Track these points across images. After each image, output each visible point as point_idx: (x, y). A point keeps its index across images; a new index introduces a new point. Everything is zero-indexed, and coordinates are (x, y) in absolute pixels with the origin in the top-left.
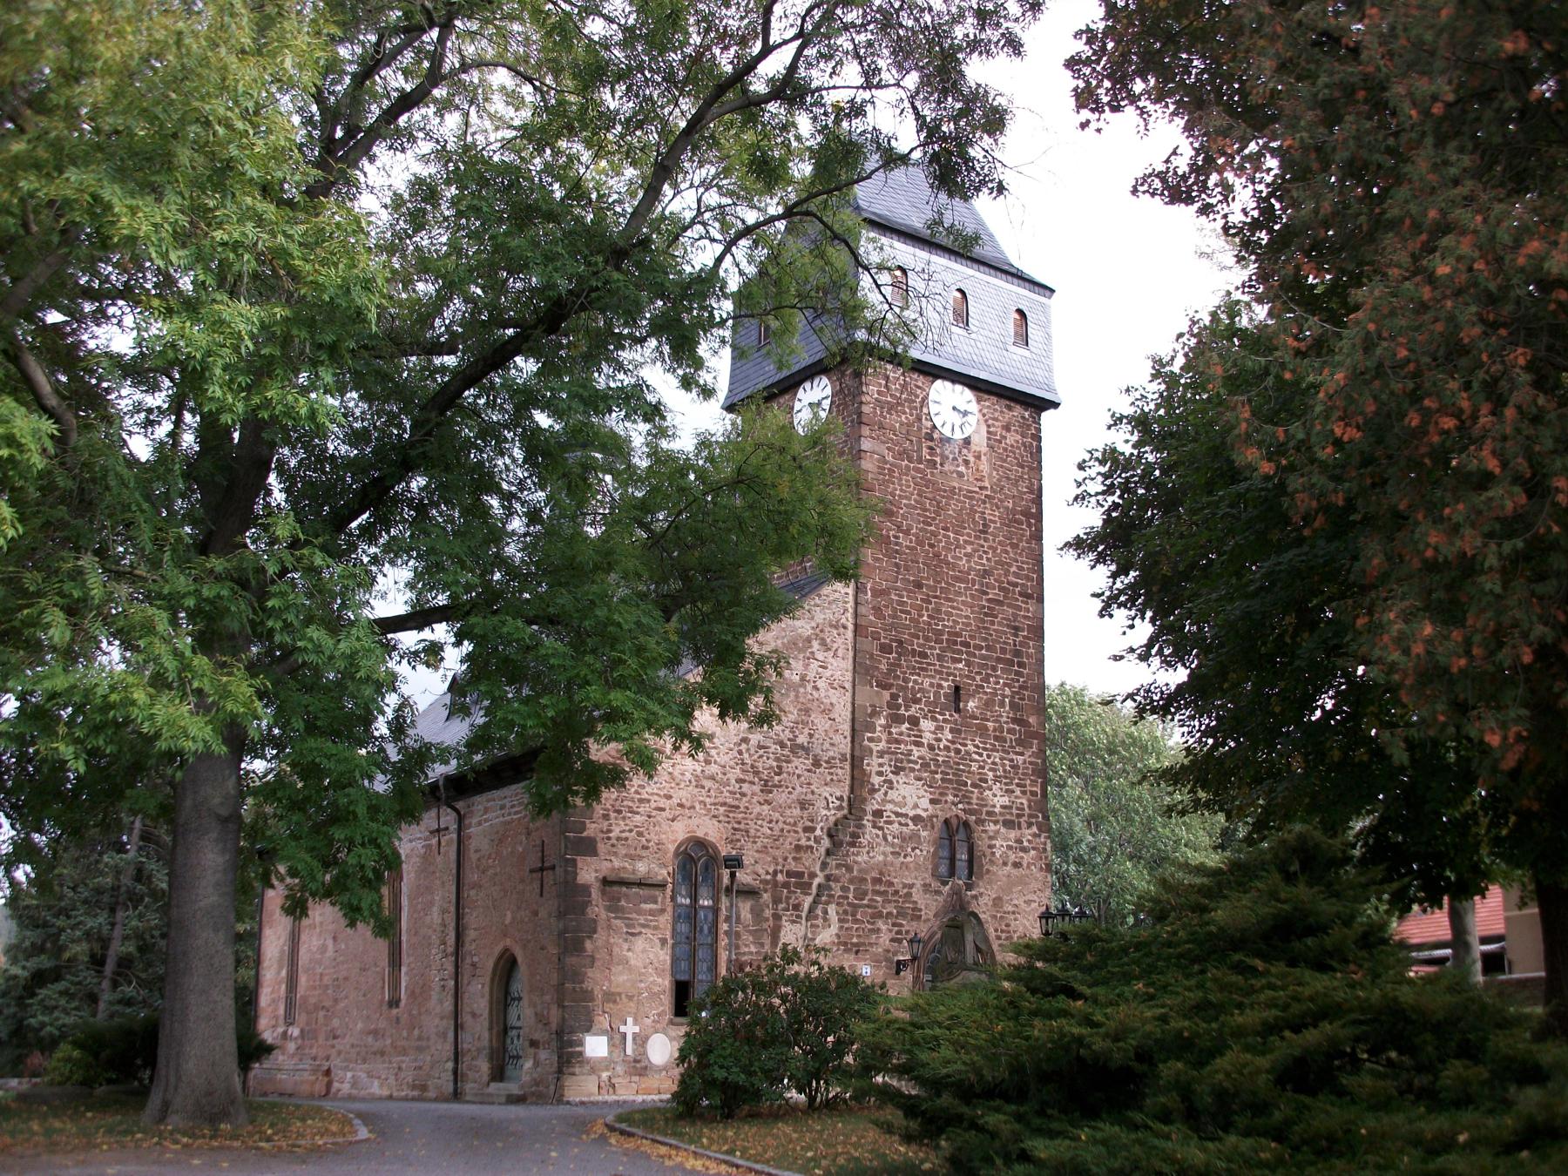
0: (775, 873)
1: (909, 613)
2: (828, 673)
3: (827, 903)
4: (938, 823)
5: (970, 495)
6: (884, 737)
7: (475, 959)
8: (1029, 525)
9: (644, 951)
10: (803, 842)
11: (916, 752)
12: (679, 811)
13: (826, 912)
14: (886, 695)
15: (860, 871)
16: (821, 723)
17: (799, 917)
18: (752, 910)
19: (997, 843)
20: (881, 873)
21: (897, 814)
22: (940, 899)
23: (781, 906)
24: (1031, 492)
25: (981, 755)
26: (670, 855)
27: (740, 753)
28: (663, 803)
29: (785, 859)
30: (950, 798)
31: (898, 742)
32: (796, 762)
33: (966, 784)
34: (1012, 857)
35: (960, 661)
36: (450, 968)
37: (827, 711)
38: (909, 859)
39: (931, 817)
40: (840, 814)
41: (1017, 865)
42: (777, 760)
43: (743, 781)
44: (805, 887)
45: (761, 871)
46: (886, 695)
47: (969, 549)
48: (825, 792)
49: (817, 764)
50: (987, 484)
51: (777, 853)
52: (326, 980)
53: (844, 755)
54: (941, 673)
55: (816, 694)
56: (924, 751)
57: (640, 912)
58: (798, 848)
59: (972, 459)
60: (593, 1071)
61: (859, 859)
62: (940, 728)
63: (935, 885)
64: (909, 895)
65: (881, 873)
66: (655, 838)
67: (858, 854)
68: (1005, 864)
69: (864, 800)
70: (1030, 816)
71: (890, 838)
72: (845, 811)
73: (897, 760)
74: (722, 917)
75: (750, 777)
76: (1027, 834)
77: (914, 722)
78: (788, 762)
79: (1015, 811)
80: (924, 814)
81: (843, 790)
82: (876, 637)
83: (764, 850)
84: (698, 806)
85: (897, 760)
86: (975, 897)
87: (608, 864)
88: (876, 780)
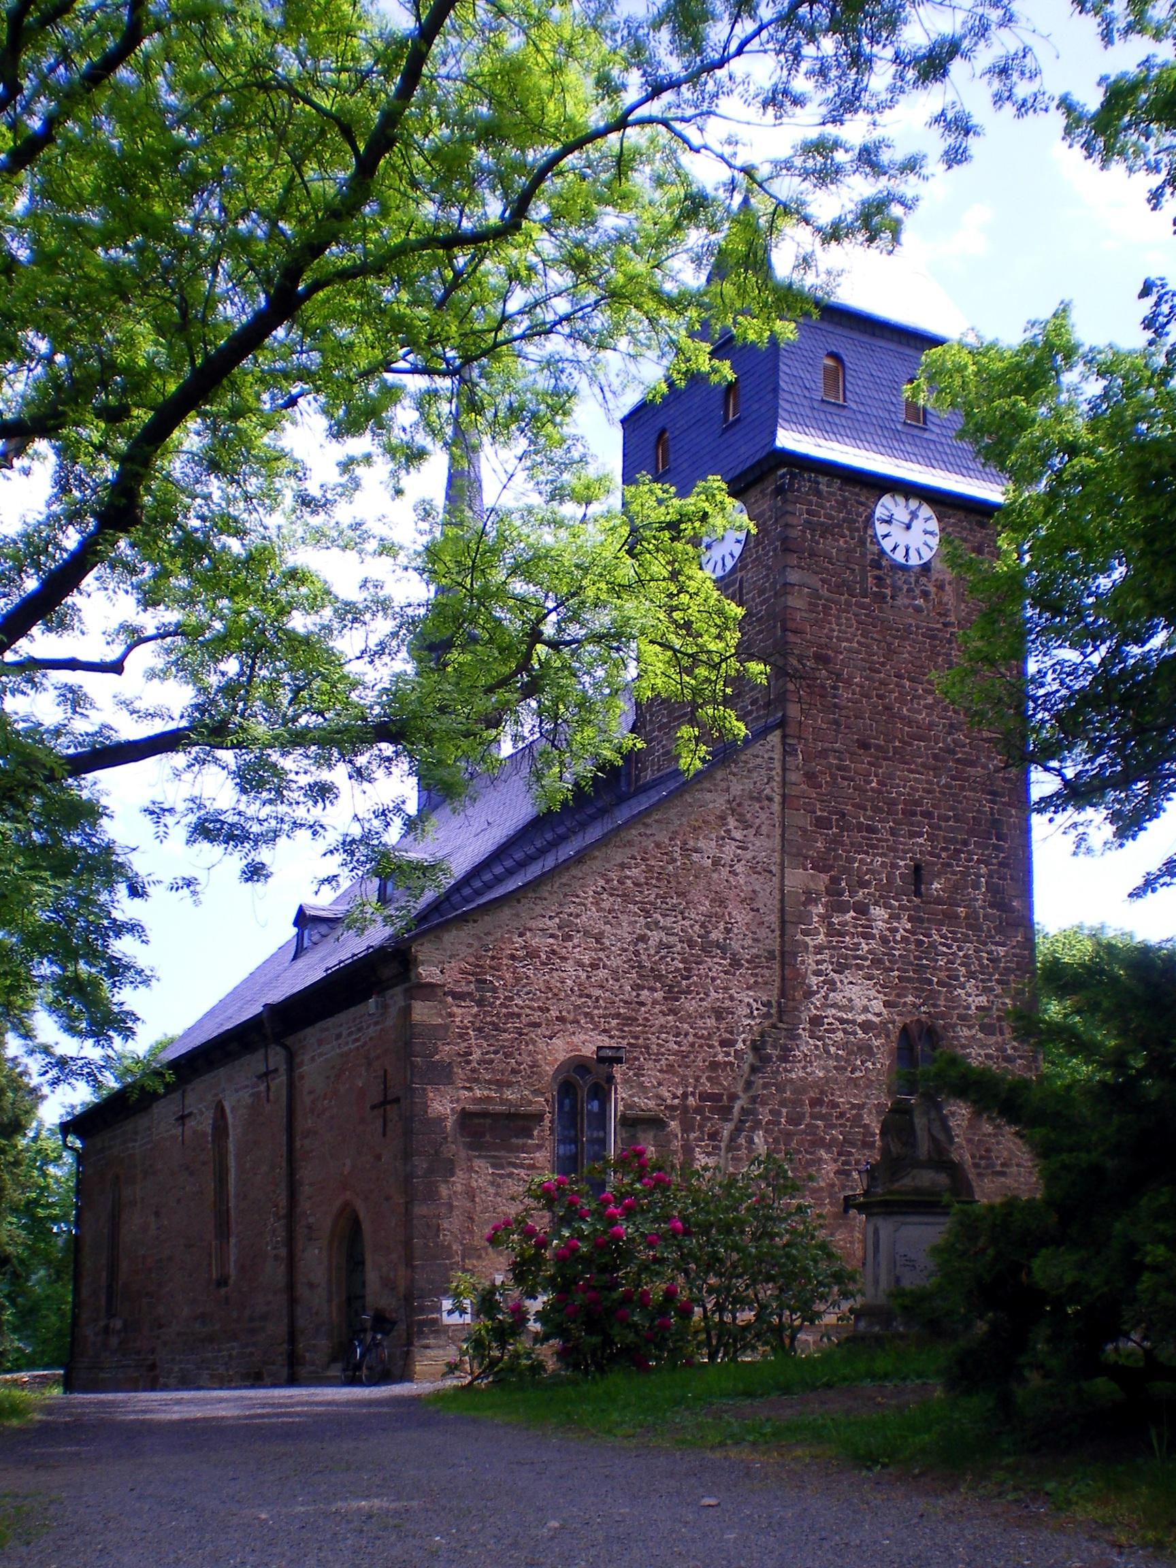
2: (749, 855)
10: (720, 1058)
14: (825, 877)
20: (822, 1092)
25: (950, 947)
28: (536, 1016)
29: (697, 1079)
30: (909, 999)
38: (858, 1074)
39: (884, 1024)
43: (643, 988)
46: (825, 877)
49: (736, 963)
53: (771, 952)
58: (714, 1066)
59: (933, 590)
65: (822, 1092)
71: (832, 1050)
73: (841, 956)
77: (862, 909)
80: (876, 1020)
88: (814, 980)
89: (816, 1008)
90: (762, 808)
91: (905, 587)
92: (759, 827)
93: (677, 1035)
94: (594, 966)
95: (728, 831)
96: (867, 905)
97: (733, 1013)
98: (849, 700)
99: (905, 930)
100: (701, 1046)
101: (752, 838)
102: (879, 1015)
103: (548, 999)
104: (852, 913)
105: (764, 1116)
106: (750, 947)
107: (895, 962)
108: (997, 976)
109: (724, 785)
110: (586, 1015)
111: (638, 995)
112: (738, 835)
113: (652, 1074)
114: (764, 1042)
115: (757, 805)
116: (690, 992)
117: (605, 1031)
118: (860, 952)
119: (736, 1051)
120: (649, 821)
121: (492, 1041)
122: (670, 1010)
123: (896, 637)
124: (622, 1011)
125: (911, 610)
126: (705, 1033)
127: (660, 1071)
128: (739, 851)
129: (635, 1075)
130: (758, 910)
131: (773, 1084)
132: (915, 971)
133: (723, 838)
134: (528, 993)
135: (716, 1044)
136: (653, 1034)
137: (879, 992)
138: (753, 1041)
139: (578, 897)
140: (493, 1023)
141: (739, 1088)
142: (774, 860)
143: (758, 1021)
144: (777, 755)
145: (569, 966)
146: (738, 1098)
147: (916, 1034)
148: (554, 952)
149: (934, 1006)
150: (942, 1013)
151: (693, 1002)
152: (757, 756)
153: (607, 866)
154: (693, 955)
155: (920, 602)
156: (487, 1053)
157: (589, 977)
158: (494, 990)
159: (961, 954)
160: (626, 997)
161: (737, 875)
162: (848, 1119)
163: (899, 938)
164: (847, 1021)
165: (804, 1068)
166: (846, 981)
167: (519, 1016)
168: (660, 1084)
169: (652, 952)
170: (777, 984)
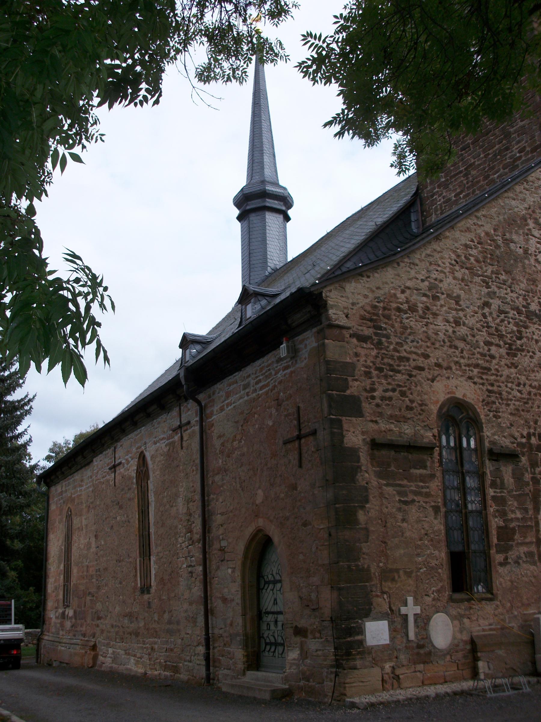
0: (529, 436)
7: (224, 543)
9: (419, 521)
26: (434, 416)
27: (484, 316)
28: (421, 362)
36: (198, 555)
42: (516, 325)
45: (517, 434)
51: (528, 416)
52: (92, 571)
57: (410, 478)
60: (375, 662)
74: (488, 482)
75: (496, 340)
78: (526, 327)
83: (516, 413)
87: (375, 427)
93: (519, 385)
94: (457, 323)
100: (535, 395)
103: (428, 347)
110: (457, 363)
111: (489, 350)
116: (523, 350)
117: (470, 378)
121: (389, 380)
122: (512, 364)
124: (480, 362)
127: (511, 414)
129: (494, 416)
134: (412, 341)
136: (503, 383)
139: (439, 266)
140: (391, 365)
145: (439, 321)
148: (427, 308)
154: (521, 321)
156: (386, 391)
157: (454, 332)
158: (388, 337)
160: (481, 350)
167: (408, 359)
169: (495, 316)
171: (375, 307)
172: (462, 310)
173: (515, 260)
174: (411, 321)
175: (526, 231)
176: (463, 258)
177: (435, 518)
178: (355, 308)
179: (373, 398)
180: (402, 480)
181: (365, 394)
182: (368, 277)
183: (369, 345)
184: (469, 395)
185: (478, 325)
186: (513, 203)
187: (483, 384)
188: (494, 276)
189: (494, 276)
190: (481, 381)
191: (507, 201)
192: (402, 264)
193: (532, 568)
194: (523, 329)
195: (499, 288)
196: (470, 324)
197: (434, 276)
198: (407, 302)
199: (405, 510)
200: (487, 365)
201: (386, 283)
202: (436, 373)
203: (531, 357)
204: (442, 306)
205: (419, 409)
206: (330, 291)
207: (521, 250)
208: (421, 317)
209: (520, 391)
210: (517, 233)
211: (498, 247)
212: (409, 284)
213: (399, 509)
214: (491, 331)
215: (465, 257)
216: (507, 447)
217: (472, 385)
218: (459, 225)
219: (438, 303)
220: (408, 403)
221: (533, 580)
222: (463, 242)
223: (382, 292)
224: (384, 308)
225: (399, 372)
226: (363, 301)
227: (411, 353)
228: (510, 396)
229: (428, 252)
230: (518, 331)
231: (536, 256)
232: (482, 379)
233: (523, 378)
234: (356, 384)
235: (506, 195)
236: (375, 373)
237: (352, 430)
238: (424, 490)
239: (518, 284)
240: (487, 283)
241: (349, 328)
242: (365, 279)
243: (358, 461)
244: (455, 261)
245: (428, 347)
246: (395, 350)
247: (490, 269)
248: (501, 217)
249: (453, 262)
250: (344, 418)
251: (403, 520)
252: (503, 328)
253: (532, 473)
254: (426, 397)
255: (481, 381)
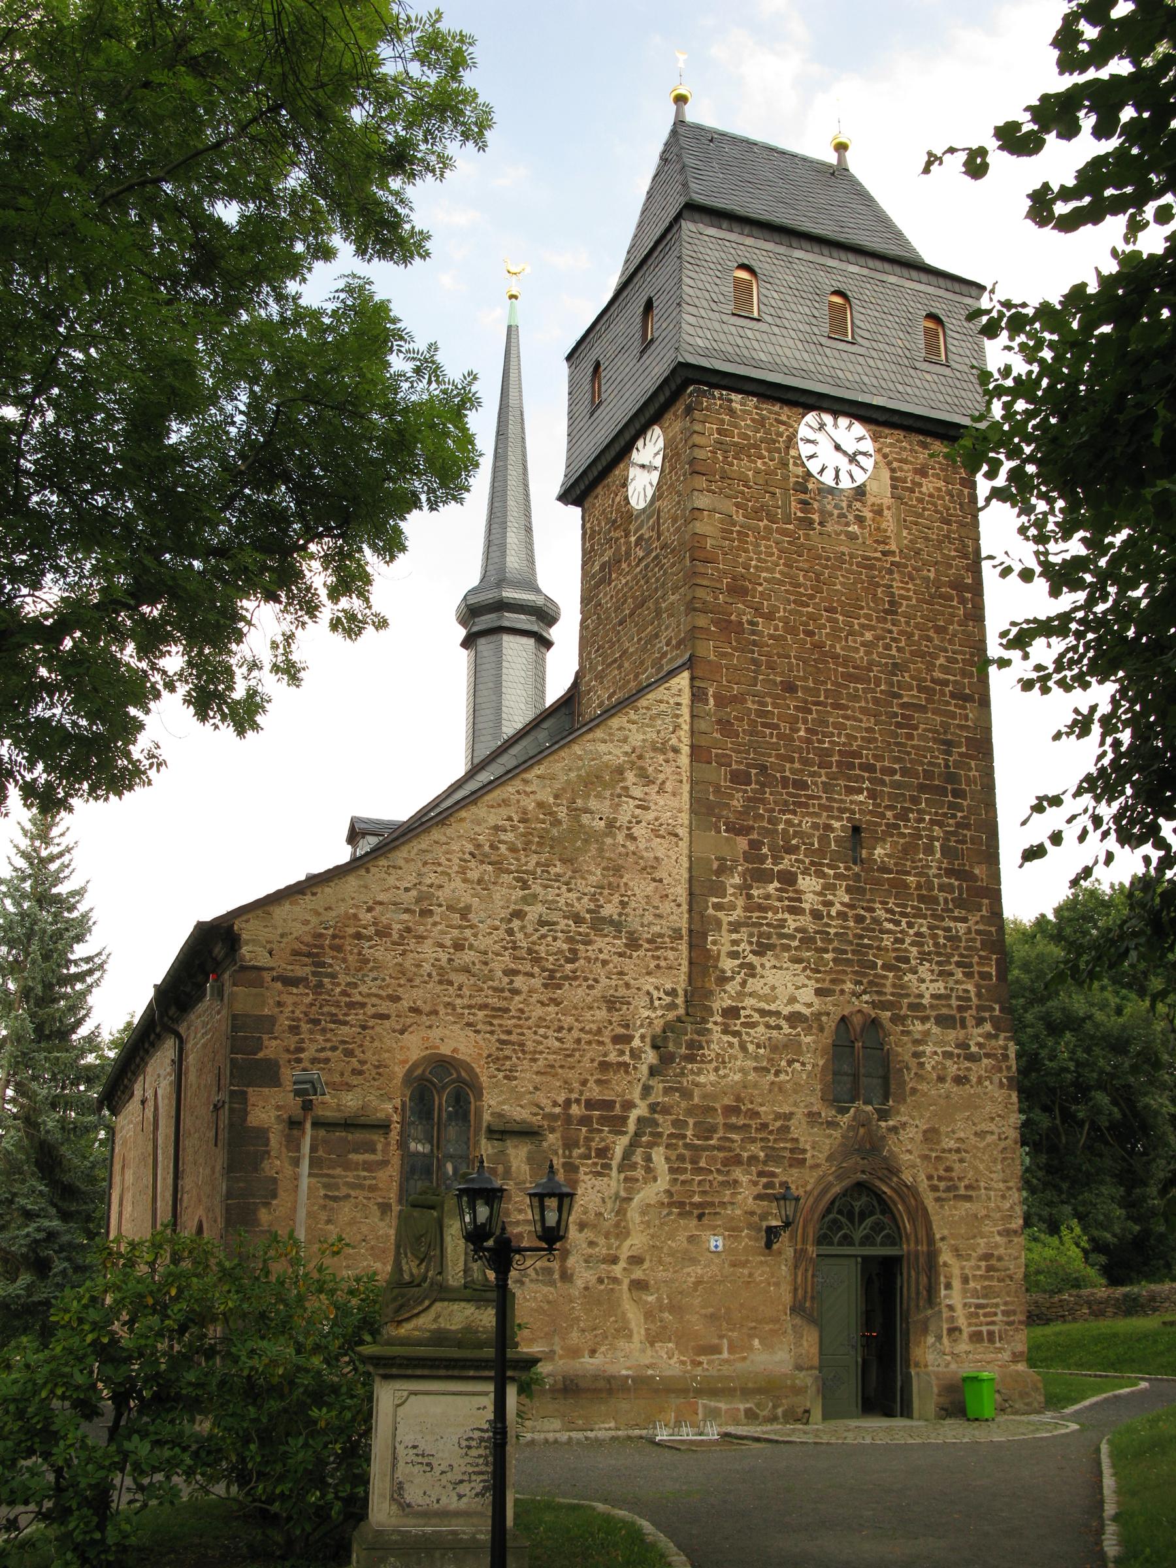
0: (568, 1103)
1: (776, 727)
2: (651, 816)
3: (651, 1145)
4: (830, 1023)
5: (868, 564)
6: (740, 902)
8: (963, 601)
10: (613, 1057)
11: (792, 923)
12: (412, 1018)
13: (648, 1159)
14: (742, 843)
15: (704, 1097)
16: (641, 887)
17: (607, 1166)
18: (530, 1160)
19: (929, 1049)
20: (738, 1099)
21: (763, 1013)
22: (837, 1134)
23: (576, 1152)
24: (965, 556)
25: (898, 923)
26: (398, 1081)
28: (385, 1007)
29: (584, 1083)
30: (848, 986)
31: (762, 908)
32: (600, 942)
33: (874, 966)
34: (952, 1069)
35: (860, 791)
37: (650, 869)
38: (783, 1077)
39: (818, 1015)
40: (671, 1016)
41: (959, 1080)
42: (570, 940)
43: (515, 972)
44: (617, 1124)
45: (544, 1102)
46: (742, 843)
47: (868, 636)
48: (648, 984)
49: (633, 943)
50: (894, 547)
51: (570, 1074)
53: (677, 931)
54: (829, 809)
55: (631, 847)
56: (805, 921)
57: (347, 1166)
58: (605, 1066)
59: (869, 515)
61: (702, 1079)
62: (832, 888)
63: (828, 1113)
64: (785, 1129)
65: (738, 1099)
66: (374, 1059)
67: (700, 1072)
68: (941, 1079)
69: (709, 994)
70: (980, 1008)
72: (681, 1011)
73: (760, 935)
76: (976, 1035)
77: (788, 879)
78: (588, 943)
79: (954, 1002)
80: (806, 1011)
81: (679, 980)
82: (723, 761)
83: (550, 1070)
84: (442, 1011)
85: (760, 935)
86: (894, 1130)
88: (728, 964)
89: (731, 997)
90: (667, 761)
91: (836, 512)
92: (663, 782)
93: (560, 1029)
94: (458, 946)
95: (626, 788)
96: (795, 875)
97: (629, 1003)
98: (771, 637)
99: (842, 904)
100: (589, 1043)
101: (654, 797)
102: (809, 1005)
103: (400, 986)
104: (776, 884)
105: (667, 1129)
106: (650, 924)
107: (830, 941)
108: (956, 958)
109: (619, 735)
111: (512, 982)
112: (637, 792)
113: (527, 1076)
114: (666, 1039)
115: (661, 758)
116: (576, 978)
117: (469, 1025)
118: (786, 931)
119: (632, 1050)
120: (527, 776)
122: (551, 999)
123: (826, 567)
124: (490, 1001)
125: (843, 537)
126: (594, 1027)
127: (538, 1073)
128: (638, 811)
129: (506, 1077)
130: (661, 881)
131: (677, 1090)
132: (854, 952)
133: (619, 796)
135: (607, 1040)
137: (809, 978)
138: (654, 1038)
141: (636, 1094)
142: (680, 821)
143: (659, 1013)
144: (685, 699)
146: (634, 1106)
147: (858, 1029)
148: (408, 930)
149: (879, 993)
150: (891, 1003)
151: (579, 991)
152: (661, 701)
153: (477, 829)
154: (580, 934)
155: (854, 528)
156: (323, 1049)
157: (450, 960)
158: (333, 976)
159: (911, 932)
160: (495, 984)
161: (635, 839)
162: (771, 1132)
163: (833, 913)
164: (770, 1013)
165: (716, 1070)
166: (768, 965)
167: (363, 1005)
168: (536, 1088)
169: (530, 930)
170: (684, 968)
171: (321, 935)
172: (471, 927)
173: (586, 841)
174: (380, 952)
175: (619, 791)
176: (487, 848)
177: (382, 1220)
178: (285, 940)
179: (299, 1061)
180: (334, 1168)
181: (287, 1056)
182: (314, 894)
183: (301, 990)
184: (462, 1048)
185: (497, 947)
186: (602, 748)
187: (492, 1033)
188: (539, 870)
189: (539, 870)
190: (489, 1028)
191: (590, 747)
192: (373, 870)
193: (546, 1289)
194: (581, 947)
195: (546, 887)
196: (482, 948)
197: (429, 882)
198: (375, 924)
199: (332, 1209)
200: (504, 1004)
201: (343, 900)
202: (409, 1021)
203: (590, 987)
204: (435, 924)
205: (374, 1072)
206: (247, 921)
207: (602, 823)
208: (394, 943)
209: (558, 1039)
210: (599, 796)
211: (557, 822)
212: (382, 897)
213: (324, 1207)
214: (518, 953)
215: (492, 846)
216: (524, 1122)
217: (472, 1034)
218: (487, 798)
219: (430, 920)
220: (356, 1065)
221: (546, 1307)
222: (492, 822)
223: (333, 914)
224: (334, 937)
225: (345, 1023)
226: (298, 930)
227: (369, 995)
228: (541, 1048)
229: (423, 846)
230: (570, 950)
231: (629, 829)
232: (491, 1024)
233: (570, 1020)
234: (274, 1043)
235: (590, 736)
236: (305, 1027)
237: (261, 1104)
238: (368, 1182)
239: (583, 878)
240: (525, 882)
241: (272, 969)
242: (308, 897)
243: (267, 1142)
244: (471, 854)
245: (400, 986)
246: (344, 993)
247: (534, 859)
248: (573, 775)
249: (467, 857)
250: (250, 1090)
251: (329, 1222)
252: (543, 948)
253: (564, 1156)
254: (387, 1055)
255: (489, 1028)
